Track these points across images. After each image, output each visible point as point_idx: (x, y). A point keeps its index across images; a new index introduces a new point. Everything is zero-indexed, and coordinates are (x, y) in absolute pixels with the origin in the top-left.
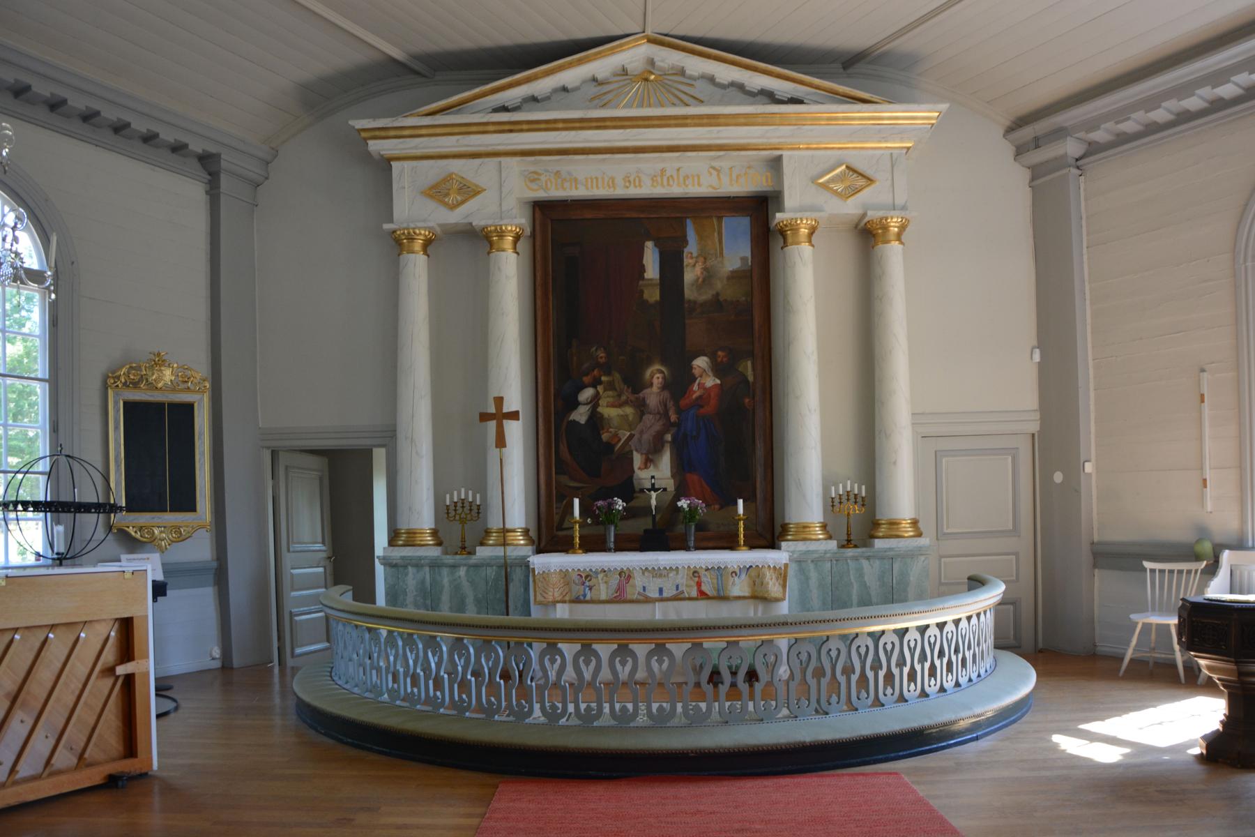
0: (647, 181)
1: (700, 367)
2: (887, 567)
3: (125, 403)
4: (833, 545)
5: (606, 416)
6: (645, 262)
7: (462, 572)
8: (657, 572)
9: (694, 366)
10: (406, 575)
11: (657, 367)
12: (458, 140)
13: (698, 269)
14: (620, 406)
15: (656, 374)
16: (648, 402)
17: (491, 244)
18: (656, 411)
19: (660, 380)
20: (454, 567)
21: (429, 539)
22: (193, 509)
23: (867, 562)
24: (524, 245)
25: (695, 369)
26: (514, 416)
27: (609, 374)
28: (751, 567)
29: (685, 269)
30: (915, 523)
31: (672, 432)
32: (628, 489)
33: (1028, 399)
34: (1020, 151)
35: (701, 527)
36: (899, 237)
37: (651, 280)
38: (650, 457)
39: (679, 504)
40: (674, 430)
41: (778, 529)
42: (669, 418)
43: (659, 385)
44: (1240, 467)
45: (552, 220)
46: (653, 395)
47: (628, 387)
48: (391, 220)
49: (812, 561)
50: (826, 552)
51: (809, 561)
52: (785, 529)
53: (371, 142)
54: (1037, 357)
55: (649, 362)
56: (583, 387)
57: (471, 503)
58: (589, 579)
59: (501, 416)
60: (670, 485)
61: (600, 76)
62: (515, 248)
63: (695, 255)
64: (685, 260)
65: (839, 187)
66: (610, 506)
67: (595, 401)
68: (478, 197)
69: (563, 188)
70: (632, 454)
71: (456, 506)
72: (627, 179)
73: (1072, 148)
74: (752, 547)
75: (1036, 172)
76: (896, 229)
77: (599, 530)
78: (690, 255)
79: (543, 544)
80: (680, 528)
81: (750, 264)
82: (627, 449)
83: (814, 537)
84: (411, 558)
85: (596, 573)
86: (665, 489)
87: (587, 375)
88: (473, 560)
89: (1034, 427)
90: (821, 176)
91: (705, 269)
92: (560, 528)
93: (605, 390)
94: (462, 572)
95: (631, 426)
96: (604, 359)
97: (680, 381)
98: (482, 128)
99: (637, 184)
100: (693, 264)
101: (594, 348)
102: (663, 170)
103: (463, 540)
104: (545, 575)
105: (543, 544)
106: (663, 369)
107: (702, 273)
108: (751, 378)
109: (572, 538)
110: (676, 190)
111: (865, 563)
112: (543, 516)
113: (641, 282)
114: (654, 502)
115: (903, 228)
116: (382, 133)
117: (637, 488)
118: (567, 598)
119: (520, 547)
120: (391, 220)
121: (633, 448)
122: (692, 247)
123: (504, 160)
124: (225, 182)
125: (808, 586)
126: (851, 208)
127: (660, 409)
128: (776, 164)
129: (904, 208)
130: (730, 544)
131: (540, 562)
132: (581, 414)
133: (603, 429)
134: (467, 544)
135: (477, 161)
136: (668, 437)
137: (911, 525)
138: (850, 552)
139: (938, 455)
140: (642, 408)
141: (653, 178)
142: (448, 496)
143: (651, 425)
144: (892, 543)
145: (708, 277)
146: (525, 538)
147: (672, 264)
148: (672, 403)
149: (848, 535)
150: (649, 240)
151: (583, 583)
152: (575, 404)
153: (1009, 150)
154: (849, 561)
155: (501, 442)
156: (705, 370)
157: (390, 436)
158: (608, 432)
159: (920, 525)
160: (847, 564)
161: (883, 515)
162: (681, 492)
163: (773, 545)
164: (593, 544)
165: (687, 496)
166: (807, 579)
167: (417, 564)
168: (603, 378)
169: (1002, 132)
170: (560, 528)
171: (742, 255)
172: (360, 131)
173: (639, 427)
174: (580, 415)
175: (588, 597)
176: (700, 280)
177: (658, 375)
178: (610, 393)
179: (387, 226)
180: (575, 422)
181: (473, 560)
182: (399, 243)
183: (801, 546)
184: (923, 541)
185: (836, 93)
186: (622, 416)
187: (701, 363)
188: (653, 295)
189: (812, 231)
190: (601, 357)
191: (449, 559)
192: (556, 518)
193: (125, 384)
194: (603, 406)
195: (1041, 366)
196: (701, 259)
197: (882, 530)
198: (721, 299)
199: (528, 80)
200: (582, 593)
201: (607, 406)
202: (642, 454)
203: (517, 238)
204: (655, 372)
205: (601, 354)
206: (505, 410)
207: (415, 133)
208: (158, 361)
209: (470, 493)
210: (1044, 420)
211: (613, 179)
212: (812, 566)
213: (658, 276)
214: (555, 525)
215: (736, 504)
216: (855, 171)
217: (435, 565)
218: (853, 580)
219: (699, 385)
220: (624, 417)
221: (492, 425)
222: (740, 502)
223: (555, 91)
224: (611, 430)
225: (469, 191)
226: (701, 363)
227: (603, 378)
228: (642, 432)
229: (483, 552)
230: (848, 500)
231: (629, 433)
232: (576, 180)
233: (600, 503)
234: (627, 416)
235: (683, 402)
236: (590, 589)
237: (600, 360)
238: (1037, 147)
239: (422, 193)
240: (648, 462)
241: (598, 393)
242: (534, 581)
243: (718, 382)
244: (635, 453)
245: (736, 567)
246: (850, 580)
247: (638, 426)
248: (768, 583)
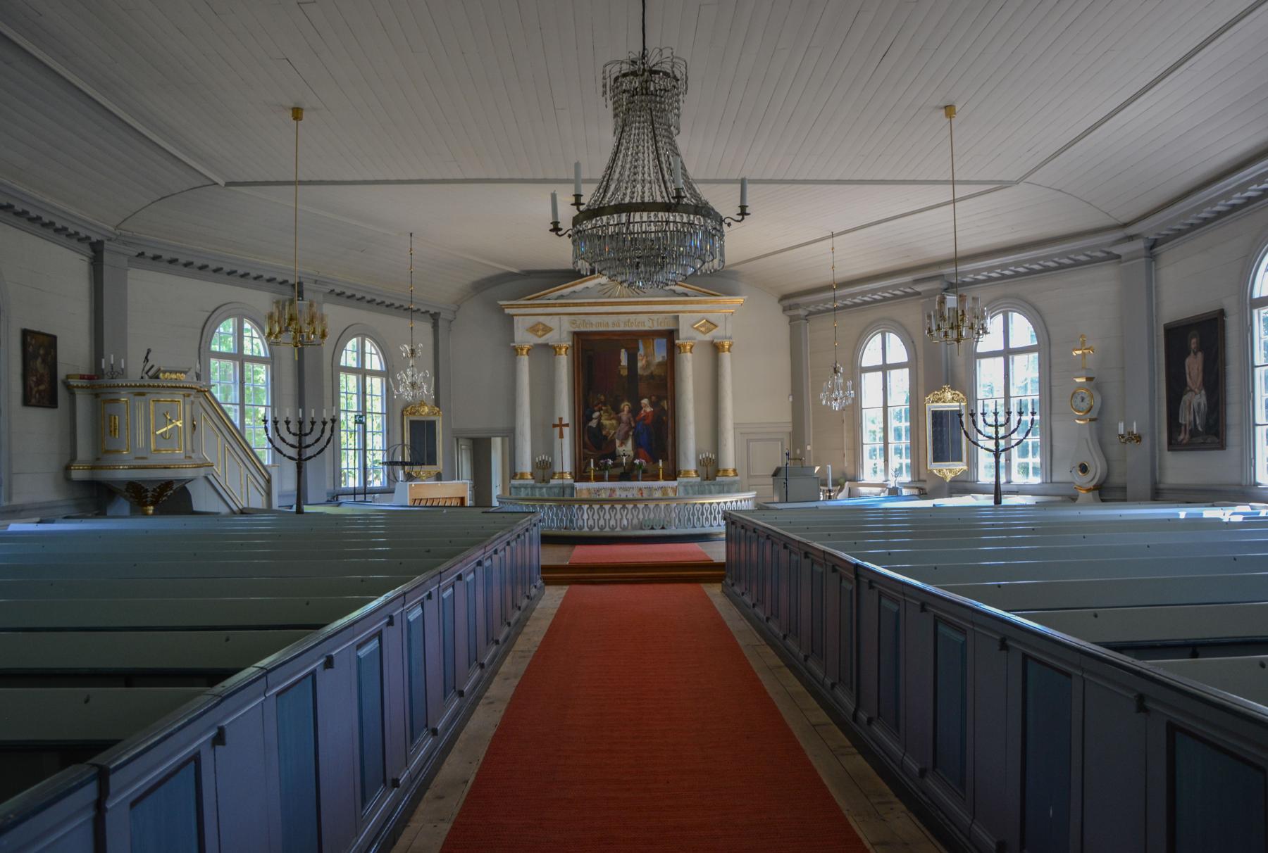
0: (622, 325)
3: (410, 421)
4: (699, 479)
7: (544, 490)
8: (625, 489)
10: (521, 491)
11: (626, 403)
13: (644, 362)
14: (611, 420)
15: (626, 406)
17: (556, 352)
20: (541, 488)
21: (529, 477)
22: (436, 464)
24: (569, 351)
26: (567, 425)
27: (605, 406)
30: (734, 470)
32: (613, 455)
33: (786, 417)
34: (785, 310)
35: (644, 472)
36: (729, 350)
39: (635, 462)
40: (633, 430)
41: (677, 473)
42: (631, 425)
44: (854, 449)
46: (625, 415)
48: (514, 342)
50: (696, 482)
52: (680, 472)
53: (506, 310)
54: (791, 399)
55: (622, 401)
56: (594, 411)
59: (561, 425)
60: (632, 454)
61: (602, 283)
62: (566, 353)
65: (702, 329)
66: (606, 463)
67: (600, 416)
68: (552, 332)
69: (587, 327)
72: (613, 324)
73: (802, 312)
74: (666, 480)
75: (792, 319)
77: (602, 473)
79: (577, 478)
80: (635, 472)
85: (601, 489)
86: (629, 456)
88: (549, 485)
89: (790, 429)
90: (696, 324)
91: (647, 361)
92: (585, 472)
94: (544, 490)
95: (615, 429)
97: (636, 409)
98: (554, 305)
102: (629, 320)
103: (544, 477)
104: (581, 490)
105: (577, 478)
106: (629, 404)
108: (666, 408)
109: (590, 476)
110: (634, 328)
111: (712, 487)
112: (577, 466)
113: (620, 367)
114: (624, 461)
115: (730, 346)
116: (512, 306)
117: (617, 454)
119: (568, 480)
120: (514, 342)
122: (641, 352)
123: (561, 316)
124: (441, 323)
126: (708, 337)
128: (677, 318)
129: (730, 338)
130: (655, 477)
131: (577, 485)
134: (545, 479)
135: (550, 317)
136: (631, 433)
138: (706, 482)
139: (748, 441)
141: (625, 323)
143: (623, 427)
144: (724, 478)
145: (648, 364)
147: (633, 359)
149: (707, 475)
150: (623, 347)
152: (591, 419)
153: (779, 308)
155: (561, 436)
157: (510, 435)
159: (737, 471)
161: (721, 467)
162: (636, 456)
163: (675, 479)
164: (599, 478)
165: (638, 458)
167: (526, 487)
168: (603, 408)
169: (777, 300)
170: (585, 472)
172: (501, 305)
173: (619, 429)
174: (593, 424)
177: (627, 407)
178: (606, 414)
179: (512, 344)
180: (591, 427)
181: (549, 485)
182: (516, 351)
183: (685, 480)
184: (737, 478)
185: (701, 291)
187: (645, 401)
188: (624, 372)
189: (692, 347)
191: (539, 485)
192: (583, 468)
193: (410, 414)
195: (793, 402)
197: (721, 473)
198: (654, 373)
199: (573, 285)
203: (567, 349)
205: (602, 398)
206: (563, 423)
207: (525, 306)
208: (422, 404)
210: (794, 427)
211: (608, 323)
212: (690, 488)
215: (659, 462)
216: (709, 322)
217: (533, 487)
221: (557, 429)
222: (661, 461)
223: (584, 289)
225: (547, 329)
226: (645, 401)
227: (603, 408)
229: (553, 482)
232: (592, 324)
233: (602, 461)
238: (790, 309)
239: (527, 330)
240: (622, 444)
242: (576, 493)
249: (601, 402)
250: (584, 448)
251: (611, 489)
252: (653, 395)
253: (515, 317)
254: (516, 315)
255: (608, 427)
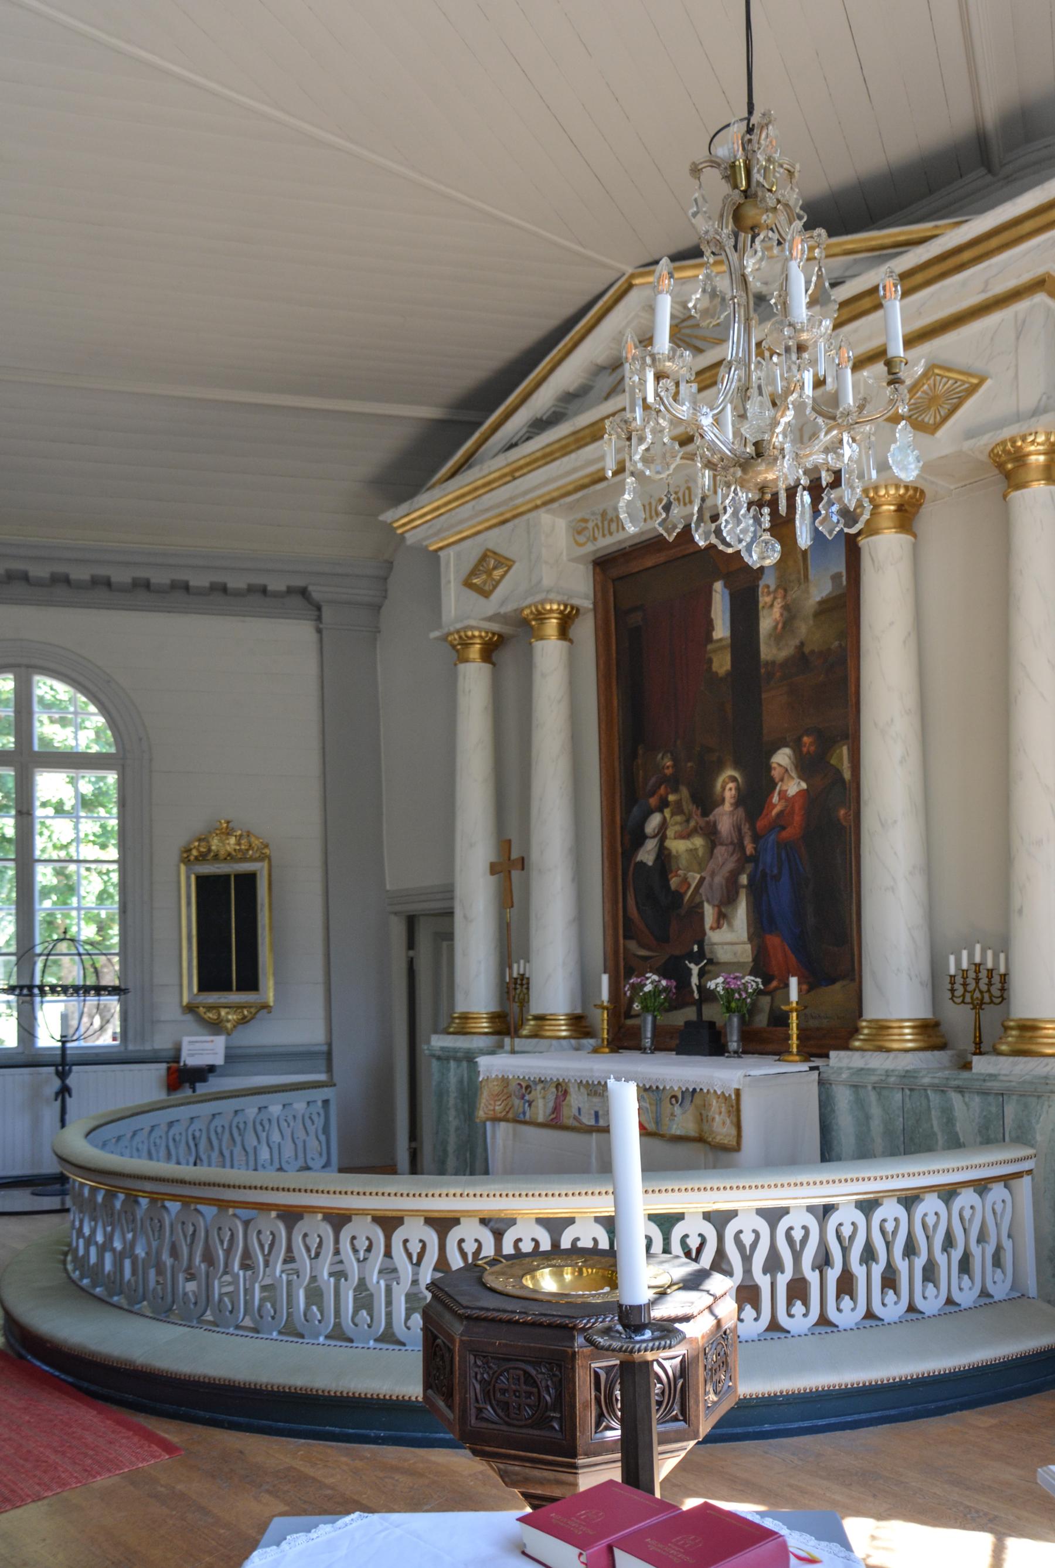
1: (779, 765)
2: (994, 1109)
5: (674, 852)
6: (713, 616)
9: (774, 765)
11: (730, 772)
12: (474, 507)
13: (777, 611)
16: (719, 827)
18: (730, 840)
19: (733, 792)
21: (484, 1025)
23: (959, 1096)
25: (775, 769)
27: (675, 790)
28: (694, 1090)
29: (761, 614)
31: (748, 871)
37: (721, 640)
38: (723, 910)
40: (749, 867)
43: (732, 801)
45: (614, 581)
46: (725, 818)
47: (697, 807)
48: (439, 625)
49: (874, 1088)
50: (888, 1073)
51: (870, 1088)
55: (720, 767)
57: (990, 972)
58: (529, 1090)
63: (772, 588)
64: (761, 599)
67: (662, 833)
70: (702, 907)
71: (965, 978)
76: (1042, 458)
78: (766, 590)
81: (844, 583)
82: (697, 900)
83: (895, 1045)
84: (456, 1050)
87: (652, 794)
91: (786, 608)
93: (673, 814)
95: (701, 866)
96: (670, 769)
99: (687, 500)
100: (770, 603)
101: (660, 756)
107: (782, 615)
111: (955, 1098)
113: (710, 647)
118: (510, 1115)
121: (704, 898)
125: (869, 1130)
127: (734, 835)
132: (648, 852)
133: (671, 872)
136: (744, 879)
137: (915, 1031)
140: (713, 838)
142: (952, 958)
143: (724, 859)
146: (570, 1028)
148: (747, 826)
151: (523, 1097)
152: (639, 838)
154: (929, 1092)
156: (787, 770)
158: (677, 875)
160: (927, 1097)
166: (868, 1117)
168: (671, 798)
171: (834, 570)
173: (711, 865)
174: (647, 855)
175: (527, 1117)
176: (780, 626)
177: (731, 785)
178: (678, 818)
180: (642, 864)
186: (691, 850)
187: (783, 758)
188: (722, 663)
190: (668, 767)
193: (196, 858)
194: (670, 839)
196: (781, 592)
198: (807, 650)
200: (521, 1110)
201: (675, 838)
202: (714, 906)
204: (727, 780)
209: (990, 953)
212: (873, 1097)
213: (728, 634)
214: (622, 1011)
215: (787, 985)
218: (936, 1128)
219: (779, 793)
220: (692, 852)
224: (680, 872)
226: (783, 758)
228: (713, 874)
230: (977, 980)
231: (698, 876)
234: (696, 849)
235: (761, 824)
236: (530, 1105)
237: (666, 771)
240: (722, 918)
241: (664, 819)
243: (804, 785)
244: (706, 905)
245: (676, 1089)
246: (932, 1127)
247: (710, 864)
248: (713, 1119)
249: (664, 780)
250: (625, 937)
251: (558, 1085)
252: (807, 732)
253: (441, 554)
254: (441, 548)
255: (683, 862)
